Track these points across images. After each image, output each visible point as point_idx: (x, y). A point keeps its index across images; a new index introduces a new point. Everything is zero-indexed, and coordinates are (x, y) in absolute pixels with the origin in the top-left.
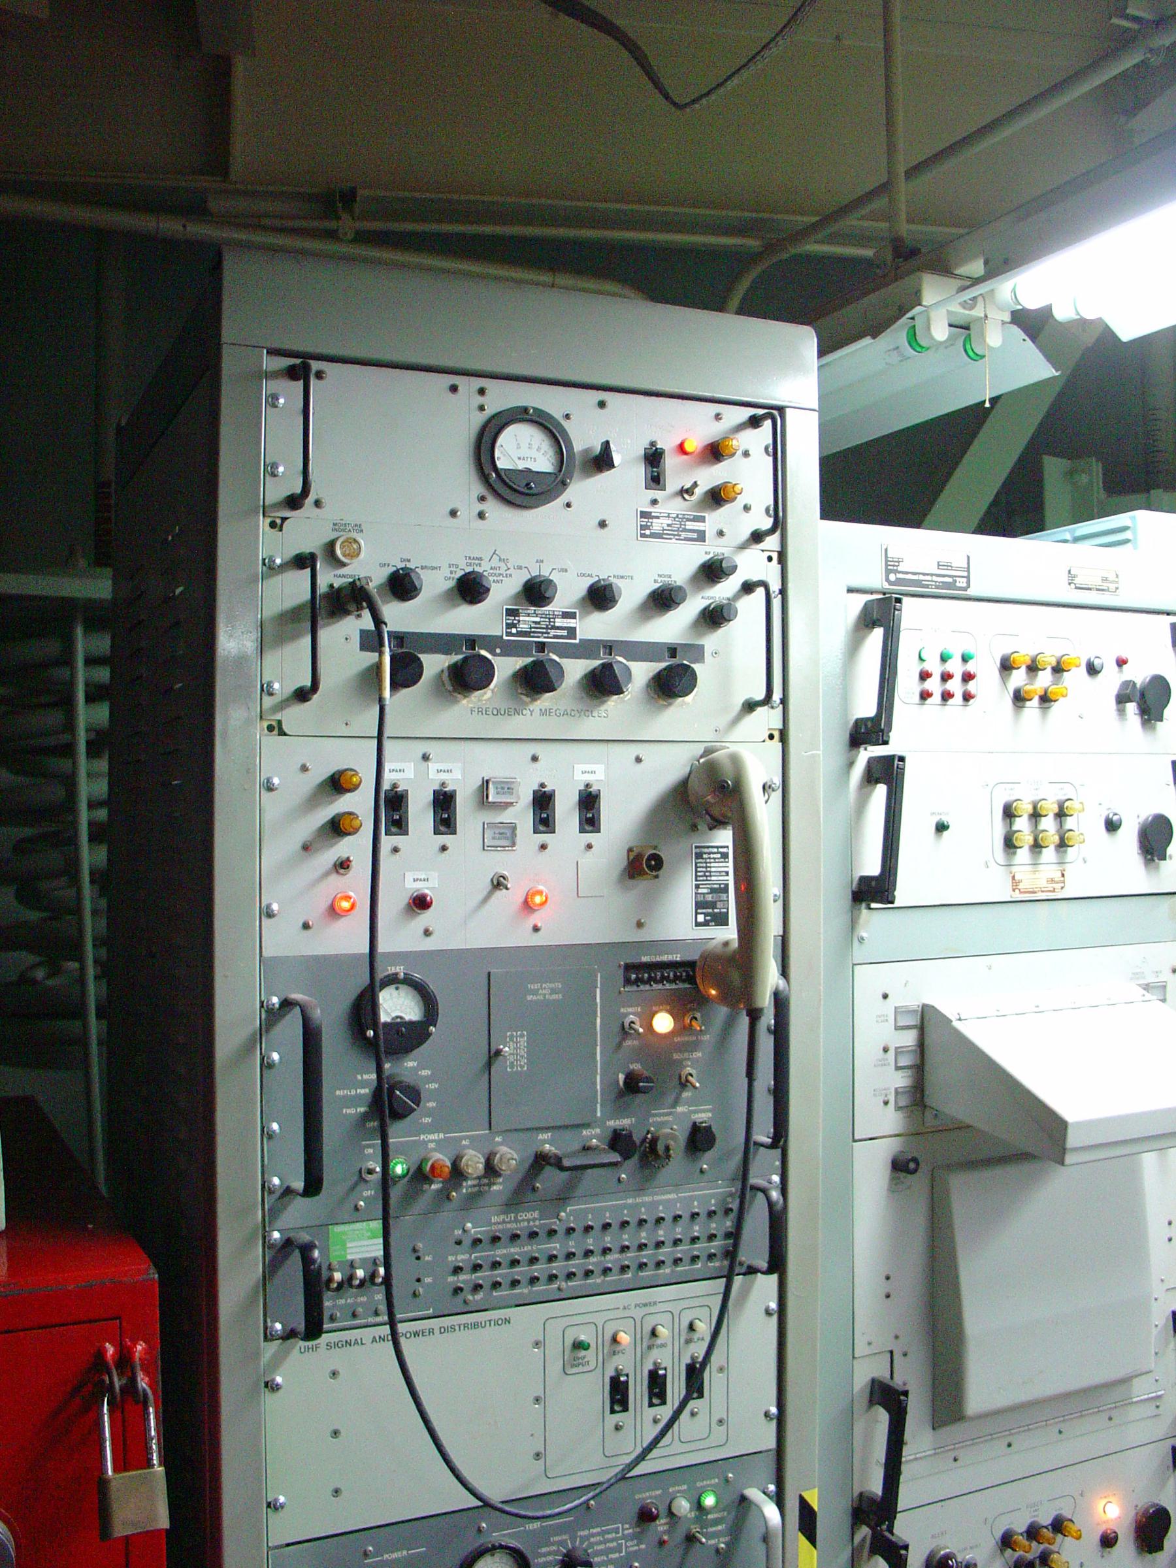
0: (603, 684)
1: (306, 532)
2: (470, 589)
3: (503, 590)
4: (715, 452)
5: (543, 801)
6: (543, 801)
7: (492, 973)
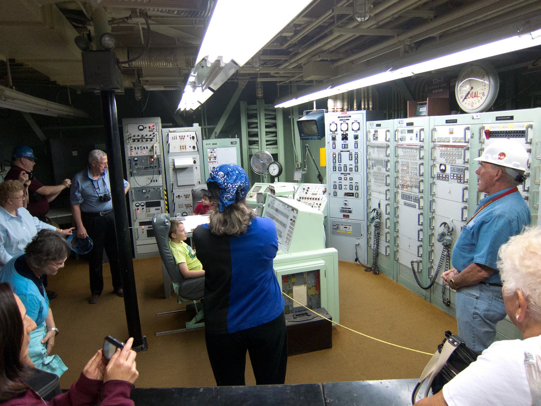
0: (147, 141)
1: (128, 134)
2: (138, 136)
3: (140, 136)
4: (153, 126)
5: (144, 148)
6: (144, 148)
7: (142, 157)
